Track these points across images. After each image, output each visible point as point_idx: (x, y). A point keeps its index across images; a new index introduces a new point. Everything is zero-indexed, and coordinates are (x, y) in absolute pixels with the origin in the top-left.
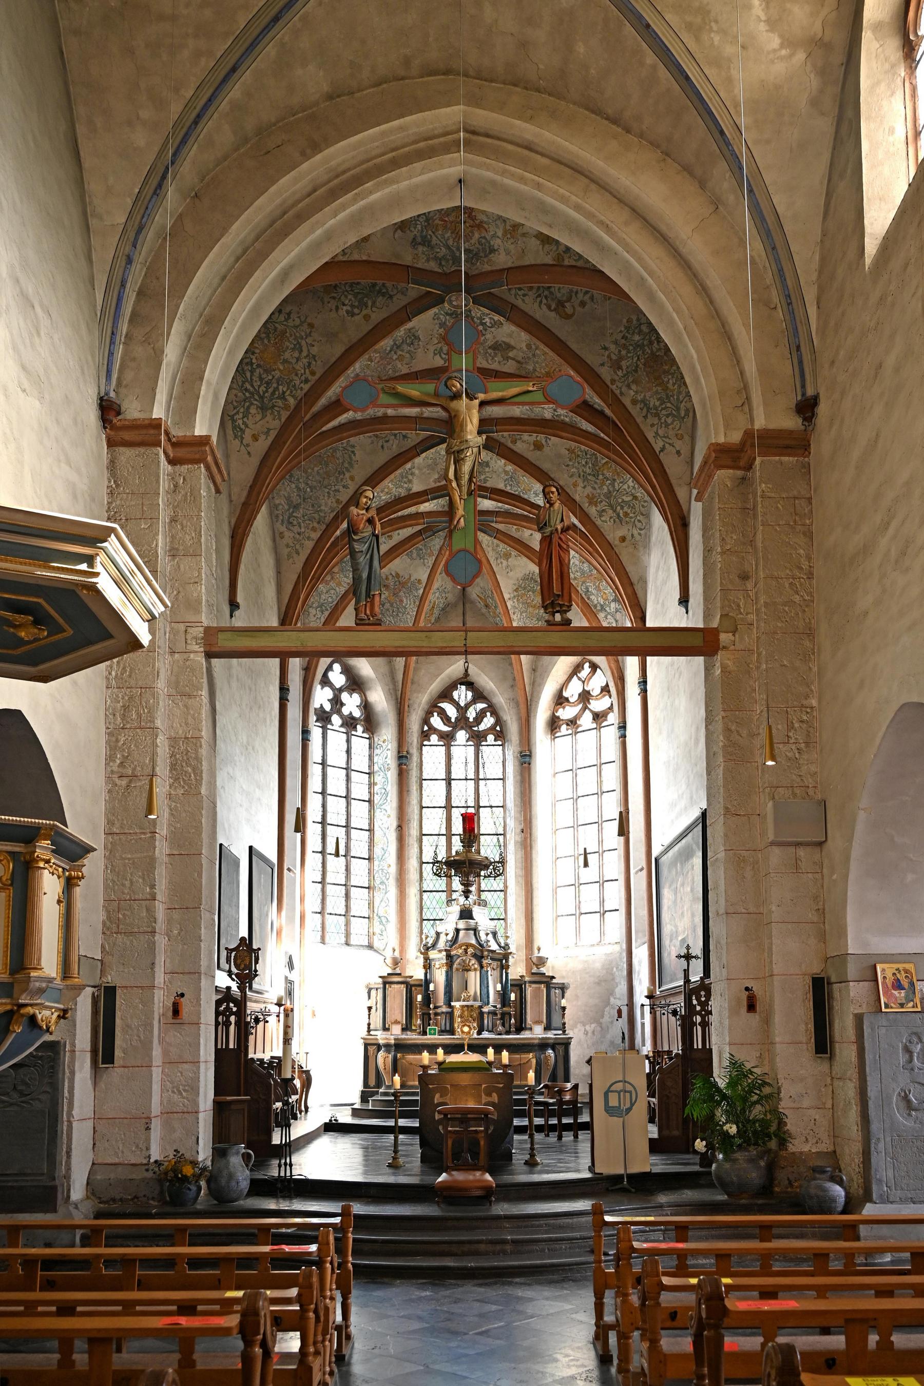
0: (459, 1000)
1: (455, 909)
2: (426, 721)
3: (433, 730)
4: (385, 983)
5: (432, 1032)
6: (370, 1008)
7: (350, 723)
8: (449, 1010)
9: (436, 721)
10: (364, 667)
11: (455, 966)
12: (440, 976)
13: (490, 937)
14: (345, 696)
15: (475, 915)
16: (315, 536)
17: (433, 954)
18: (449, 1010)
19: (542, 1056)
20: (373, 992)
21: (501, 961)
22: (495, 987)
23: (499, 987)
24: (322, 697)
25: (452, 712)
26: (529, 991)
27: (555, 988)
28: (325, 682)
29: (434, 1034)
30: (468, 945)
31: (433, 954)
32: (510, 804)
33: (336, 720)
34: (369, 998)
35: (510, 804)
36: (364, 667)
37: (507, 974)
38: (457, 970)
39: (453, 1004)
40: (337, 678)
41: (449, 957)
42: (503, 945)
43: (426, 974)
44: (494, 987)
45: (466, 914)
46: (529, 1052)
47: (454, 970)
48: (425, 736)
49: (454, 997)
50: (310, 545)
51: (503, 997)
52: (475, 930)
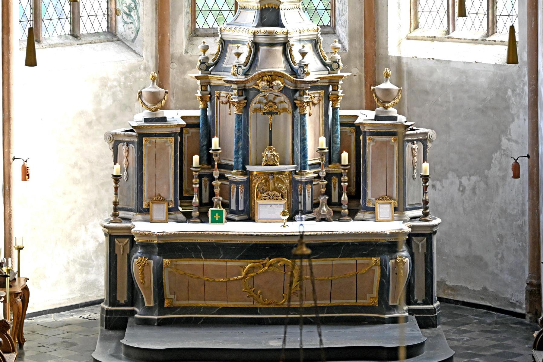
0: (259, 164)
4: (141, 136)
5: (217, 217)
6: (116, 178)
8: (244, 178)
11: (253, 106)
12: (228, 117)
13: (308, 48)
18: (244, 178)
19: (391, 263)
20: (122, 148)
21: (326, 88)
22: (317, 142)
23: (323, 142)
26: (371, 146)
27: (412, 142)
29: (220, 221)
34: (115, 162)
37: (335, 110)
38: (256, 110)
39: (248, 168)
42: (328, 61)
43: (204, 111)
44: (315, 142)
46: (371, 255)
47: (251, 113)
49: (252, 157)
51: (330, 156)
52: (285, 45)
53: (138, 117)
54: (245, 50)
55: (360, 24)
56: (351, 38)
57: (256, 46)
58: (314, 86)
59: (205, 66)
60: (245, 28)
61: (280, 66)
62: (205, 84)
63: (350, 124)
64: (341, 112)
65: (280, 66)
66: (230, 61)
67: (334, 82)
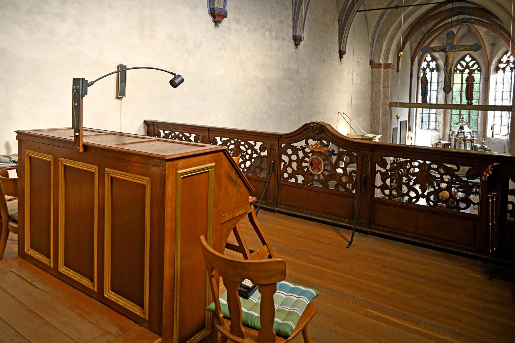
1: (458, 126)
2: (456, 67)
3: (458, 69)
7: (432, 70)
9: (459, 67)
10: (436, 55)
14: (431, 63)
15: (464, 128)
16: (421, 37)
17: (451, 137)
24: (424, 65)
25: (464, 64)
28: (425, 60)
30: (461, 138)
31: (451, 137)
32: (481, 91)
33: (428, 70)
35: (481, 91)
36: (436, 55)
40: (429, 58)
41: (455, 139)
45: (462, 128)
48: (455, 71)
50: (419, 39)
52: (464, 133)
53: (437, 142)
54: (456, 133)
55: (482, 131)
56: (480, 133)
57: (458, 133)
58: (469, 140)
59: (449, 135)
60: (456, 130)
61: (463, 136)
62: (449, 138)
63: (475, 146)
64: (475, 145)
65: (463, 136)
66: (454, 135)
67: (473, 140)
